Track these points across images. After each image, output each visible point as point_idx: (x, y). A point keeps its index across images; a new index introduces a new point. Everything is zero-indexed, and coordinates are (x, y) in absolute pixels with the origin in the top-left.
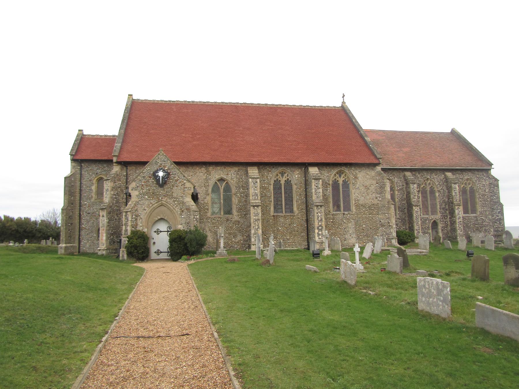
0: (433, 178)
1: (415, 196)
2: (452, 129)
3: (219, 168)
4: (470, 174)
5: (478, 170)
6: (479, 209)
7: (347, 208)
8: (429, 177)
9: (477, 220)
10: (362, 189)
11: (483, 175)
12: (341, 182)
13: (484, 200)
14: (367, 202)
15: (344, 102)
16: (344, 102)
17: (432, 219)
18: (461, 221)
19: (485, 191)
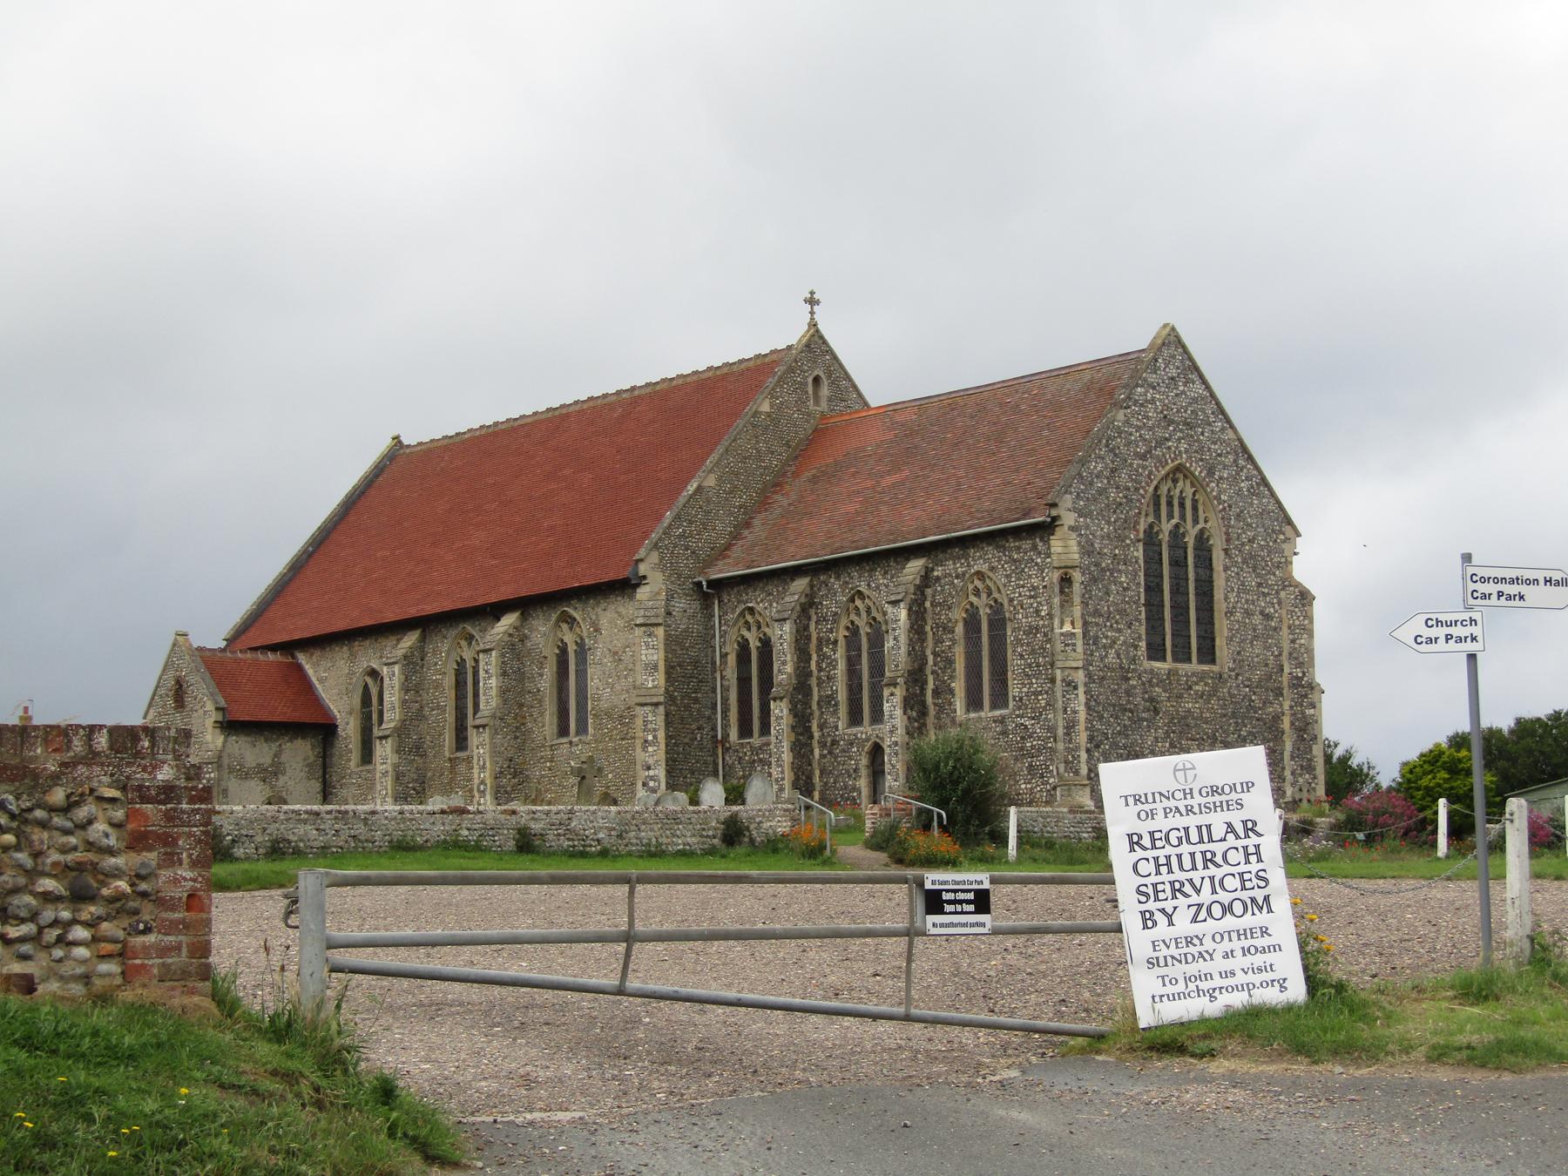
0: (877, 587)
1: (784, 663)
2: (1165, 326)
3: (367, 642)
4: (991, 551)
5: (1017, 532)
6: (1014, 690)
7: (582, 729)
8: (863, 588)
9: (1005, 733)
10: (607, 660)
11: (1034, 547)
12: (571, 648)
13: (1033, 652)
14: (616, 701)
15: (813, 324)
16: (813, 324)
17: (867, 740)
18: (896, 744)
19: (1037, 611)
